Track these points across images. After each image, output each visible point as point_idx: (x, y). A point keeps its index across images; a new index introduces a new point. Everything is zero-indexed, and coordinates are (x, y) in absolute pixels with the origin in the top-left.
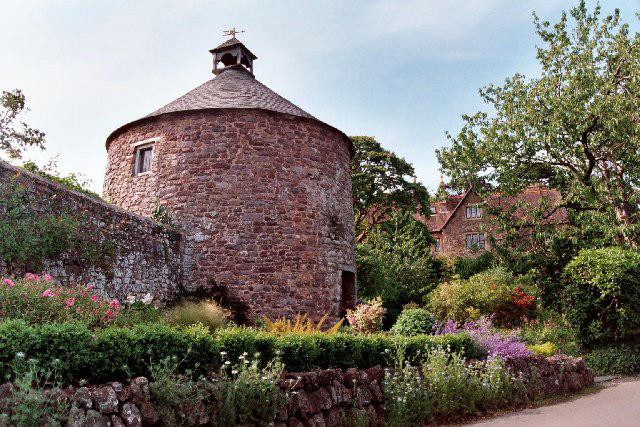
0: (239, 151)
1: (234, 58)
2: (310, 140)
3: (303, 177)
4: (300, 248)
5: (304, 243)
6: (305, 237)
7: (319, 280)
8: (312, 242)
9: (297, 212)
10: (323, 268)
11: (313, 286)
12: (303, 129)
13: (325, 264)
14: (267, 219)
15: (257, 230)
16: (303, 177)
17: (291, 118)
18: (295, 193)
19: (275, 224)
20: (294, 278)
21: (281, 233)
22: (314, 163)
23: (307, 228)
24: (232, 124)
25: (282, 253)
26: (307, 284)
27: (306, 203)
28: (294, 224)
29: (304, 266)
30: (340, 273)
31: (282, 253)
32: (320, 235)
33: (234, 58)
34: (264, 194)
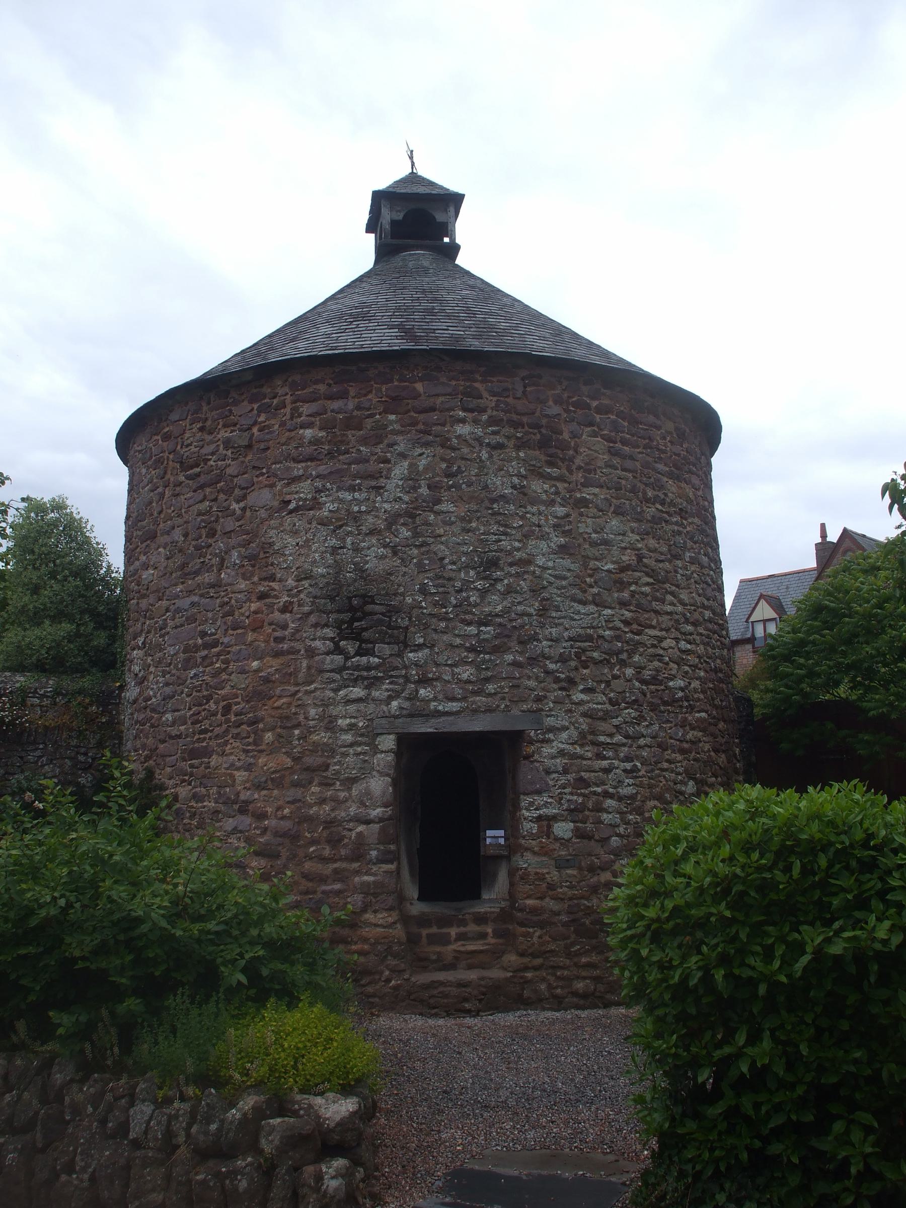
0: (168, 493)
1: (414, 219)
2: (295, 413)
3: (272, 512)
4: (260, 693)
5: (267, 680)
6: (276, 663)
7: (314, 769)
8: (289, 676)
9: (254, 606)
10: (322, 737)
11: (296, 785)
12: (282, 389)
13: (330, 725)
14: (203, 634)
15: (188, 664)
16: (272, 512)
18: (252, 558)
19: (215, 644)
20: (249, 768)
21: (226, 662)
22: (298, 469)
23: (277, 640)
24: (159, 437)
25: (227, 709)
26: (278, 783)
27: (272, 578)
28: (250, 637)
29: (269, 736)
30: (388, 742)
31: (227, 709)
32: (311, 653)
33: (414, 219)
34: (199, 579)
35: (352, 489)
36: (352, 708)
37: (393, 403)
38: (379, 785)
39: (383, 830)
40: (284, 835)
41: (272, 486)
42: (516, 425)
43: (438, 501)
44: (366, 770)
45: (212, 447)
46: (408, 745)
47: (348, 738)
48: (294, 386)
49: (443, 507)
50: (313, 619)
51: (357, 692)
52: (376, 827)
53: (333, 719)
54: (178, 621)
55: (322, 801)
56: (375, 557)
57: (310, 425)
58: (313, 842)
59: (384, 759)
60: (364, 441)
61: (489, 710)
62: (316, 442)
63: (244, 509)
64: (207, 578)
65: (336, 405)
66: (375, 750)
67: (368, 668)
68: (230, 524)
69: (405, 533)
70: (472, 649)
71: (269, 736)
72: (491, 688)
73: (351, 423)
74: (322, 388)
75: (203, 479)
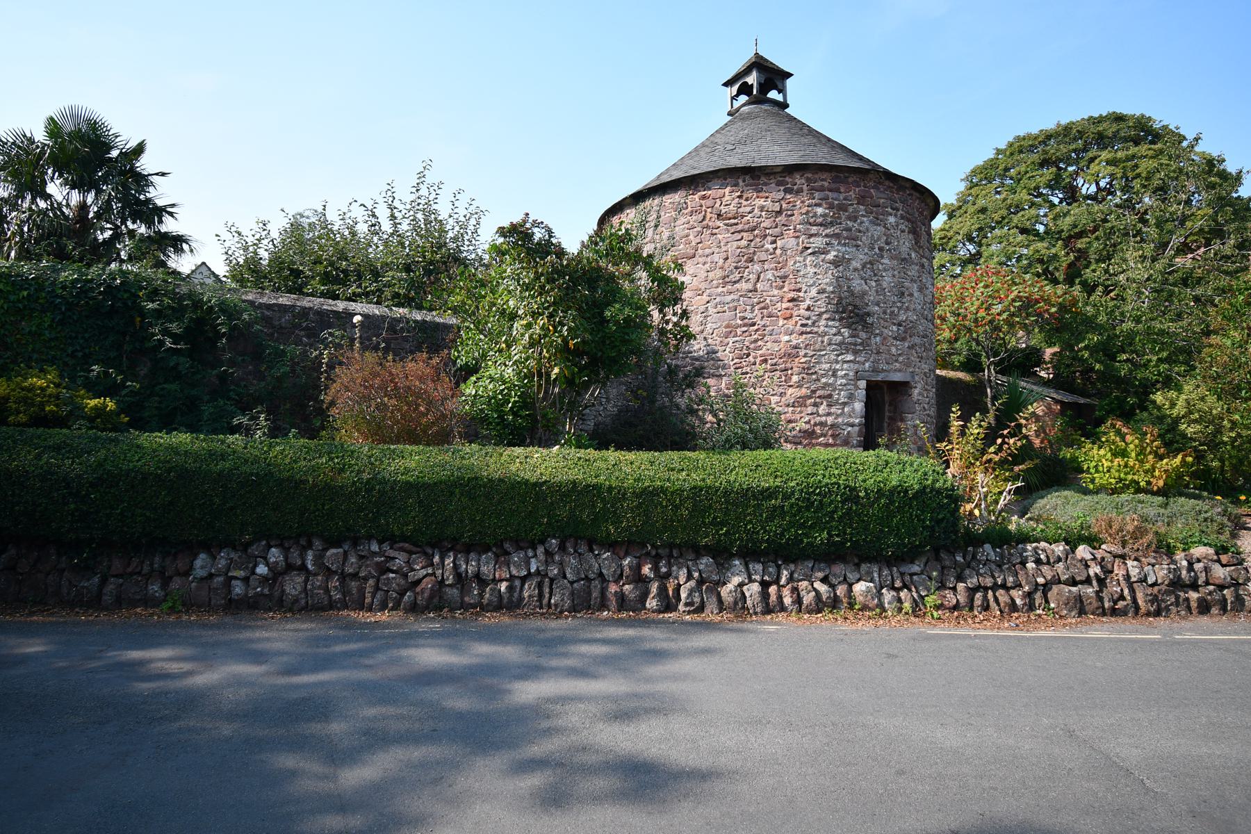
1: (763, 82)
12: (799, 181)
13: (834, 375)
17: (779, 170)
22: (814, 229)
25: (765, 361)
27: (799, 290)
33: (763, 82)
34: (737, 286)
35: (845, 245)
36: (845, 366)
37: (861, 200)
38: (859, 406)
39: (860, 431)
40: (805, 431)
41: (798, 237)
42: (909, 220)
43: (882, 257)
44: (851, 397)
45: (749, 209)
46: (872, 388)
47: (844, 381)
48: (808, 180)
49: (886, 261)
50: (825, 316)
51: (850, 357)
52: (857, 429)
53: (835, 371)
54: (719, 309)
55: (829, 414)
56: (857, 285)
57: (819, 205)
58: (822, 435)
59: (861, 393)
60: (849, 218)
61: (900, 371)
62: (824, 216)
63: (775, 249)
64: (744, 286)
65: (835, 195)
66: (857, 388)
67: (855, 345)
68: (763, 256)
69: (869, 272)
70: (895, 338)
71: (795, 378)
72: (901, 359)
73: (842, 208)
74: (826, 184)
75: (740, 227)
